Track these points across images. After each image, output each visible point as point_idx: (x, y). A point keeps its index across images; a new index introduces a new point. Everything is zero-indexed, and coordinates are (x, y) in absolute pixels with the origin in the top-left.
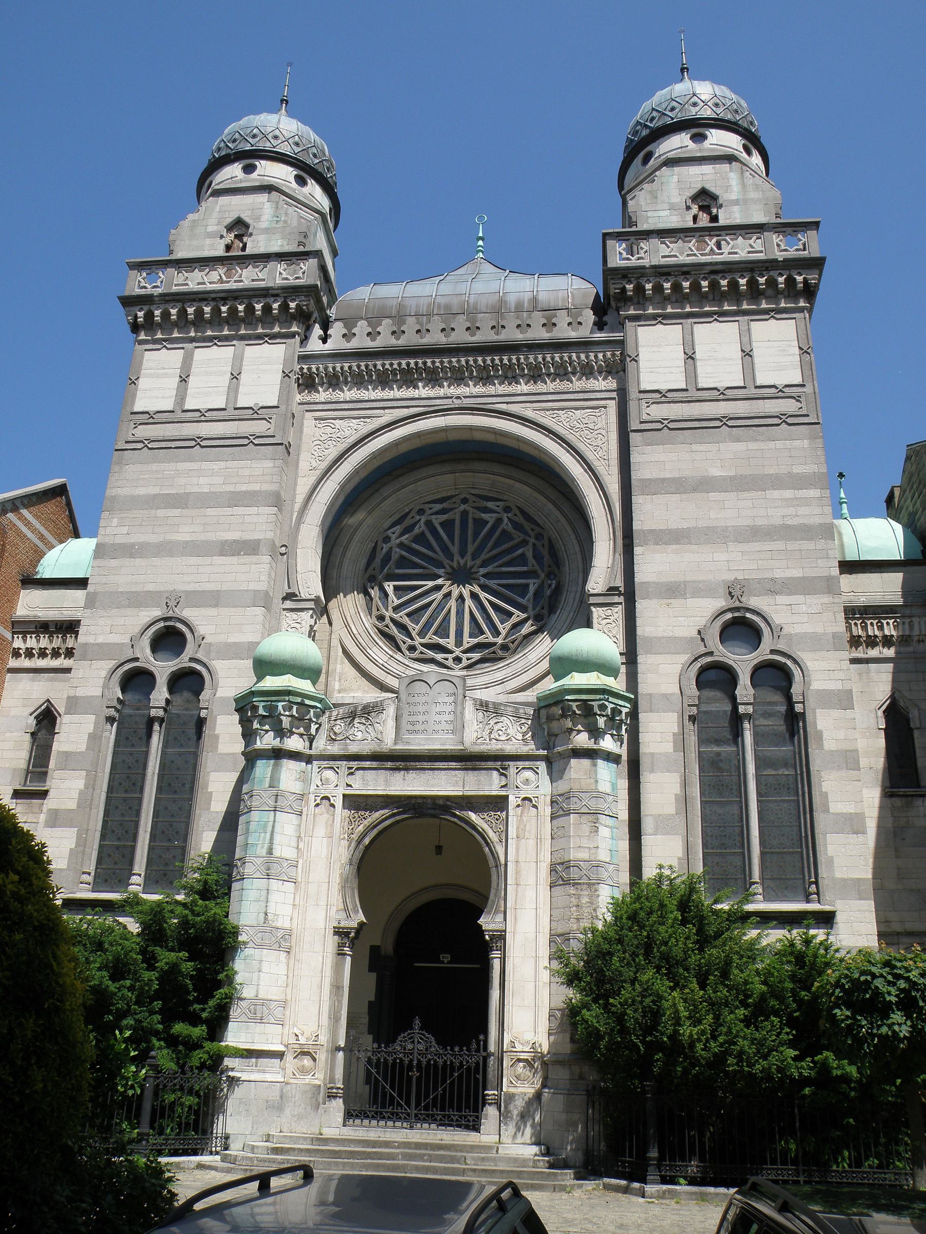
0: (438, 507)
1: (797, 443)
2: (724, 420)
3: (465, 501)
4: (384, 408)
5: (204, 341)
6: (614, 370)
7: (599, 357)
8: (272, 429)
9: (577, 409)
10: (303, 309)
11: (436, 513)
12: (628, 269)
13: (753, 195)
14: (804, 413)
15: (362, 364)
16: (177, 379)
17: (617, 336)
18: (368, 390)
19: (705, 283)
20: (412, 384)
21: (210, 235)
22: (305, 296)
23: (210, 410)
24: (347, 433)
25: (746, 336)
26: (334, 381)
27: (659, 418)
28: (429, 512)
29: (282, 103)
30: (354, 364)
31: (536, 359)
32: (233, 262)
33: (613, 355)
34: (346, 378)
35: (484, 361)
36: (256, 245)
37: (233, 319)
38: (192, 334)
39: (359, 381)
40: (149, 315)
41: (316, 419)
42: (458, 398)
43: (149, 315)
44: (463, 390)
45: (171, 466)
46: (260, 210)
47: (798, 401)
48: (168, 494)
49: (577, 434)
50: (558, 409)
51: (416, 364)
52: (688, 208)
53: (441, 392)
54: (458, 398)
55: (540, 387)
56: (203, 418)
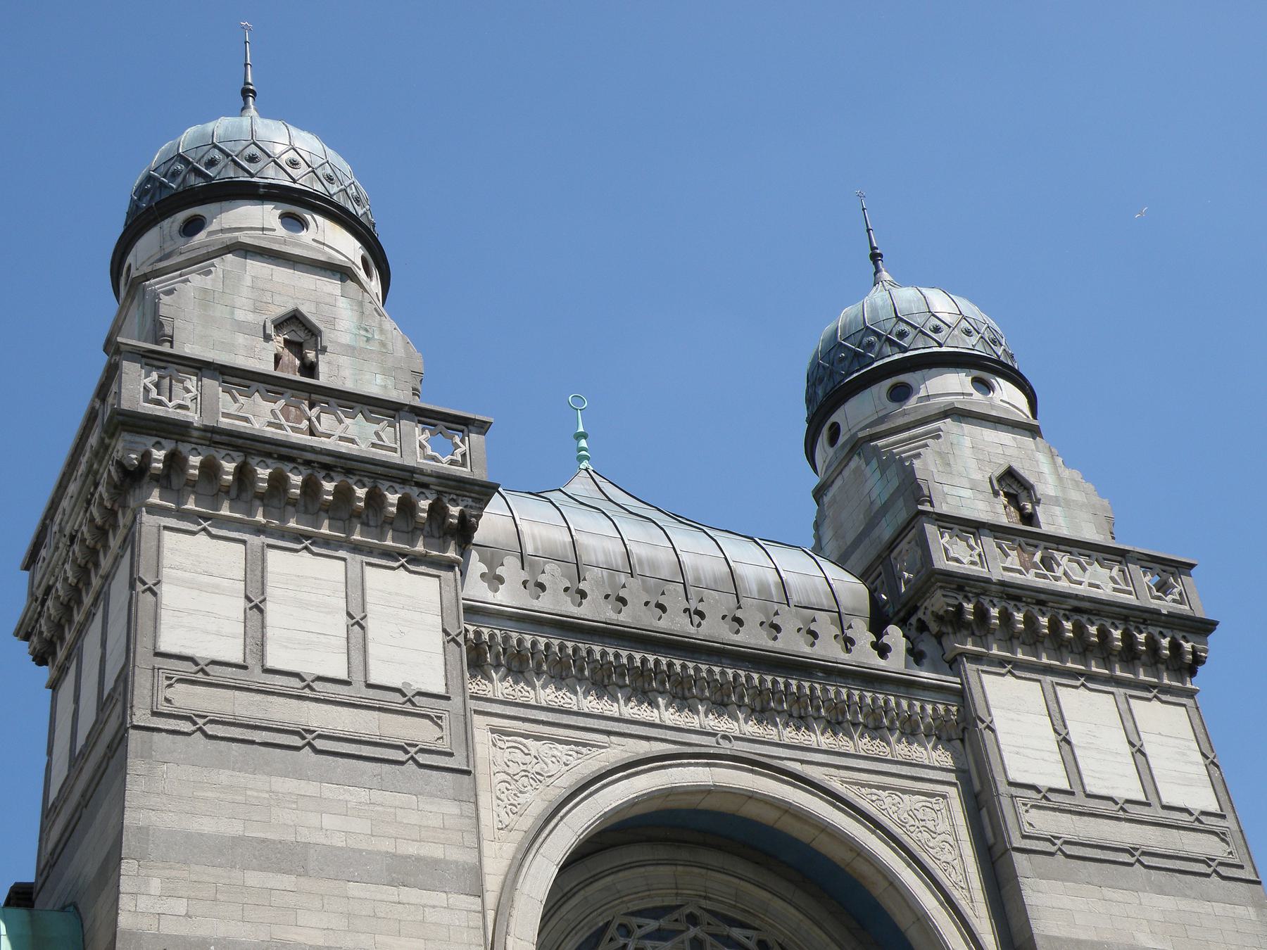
0: (652, 925)
1: (1240, 910)
2: (1136, 855)
3: (693, 920)
4: (609, 733)
5: (282, 537)
6: (944, 736)
7: (929, 709)
8: (447, 739)
9: (904, 791)
10: (429, 519)
11: (648, 936)
12: (967, 578)
13: (1075, 495)
14: (1237, 861)
15: (570, 644)
16: (241, 603)
17: (952, 681)
18: (575, 693)
19: (1068, 625)
20: (644, 695)
21: (241, 327)
22: (474, 499)
23: (320, 679)
24: (553, 768)
25: (1127, 719)
26: (519, 665)
27: (1047, 834)
28: (639, 933)
29: (245, 97)
30: (556, 642)
31: (838, 693)
32: (332, 401)
33: (947, 711)
34: (539, 665)
35: (762, 681)
36: (335, 371)
37: (341, 509)
38: (260, 518)
39: (561, 673)
40: (175, 461)
41: (493, 731)
42: (725, 737)
43: (175, 461)
44: (723, 725)
45: (260, 781)
46: (340, 312)
47: (1223, 840)
48: (264, 841)
49: (913, 835)
50: (878, 788)
51: (670, 665)
52: (996, 494)
53: (695, 722)
54: (725, 737)
55: (843, 743)
56: (307, 692)
